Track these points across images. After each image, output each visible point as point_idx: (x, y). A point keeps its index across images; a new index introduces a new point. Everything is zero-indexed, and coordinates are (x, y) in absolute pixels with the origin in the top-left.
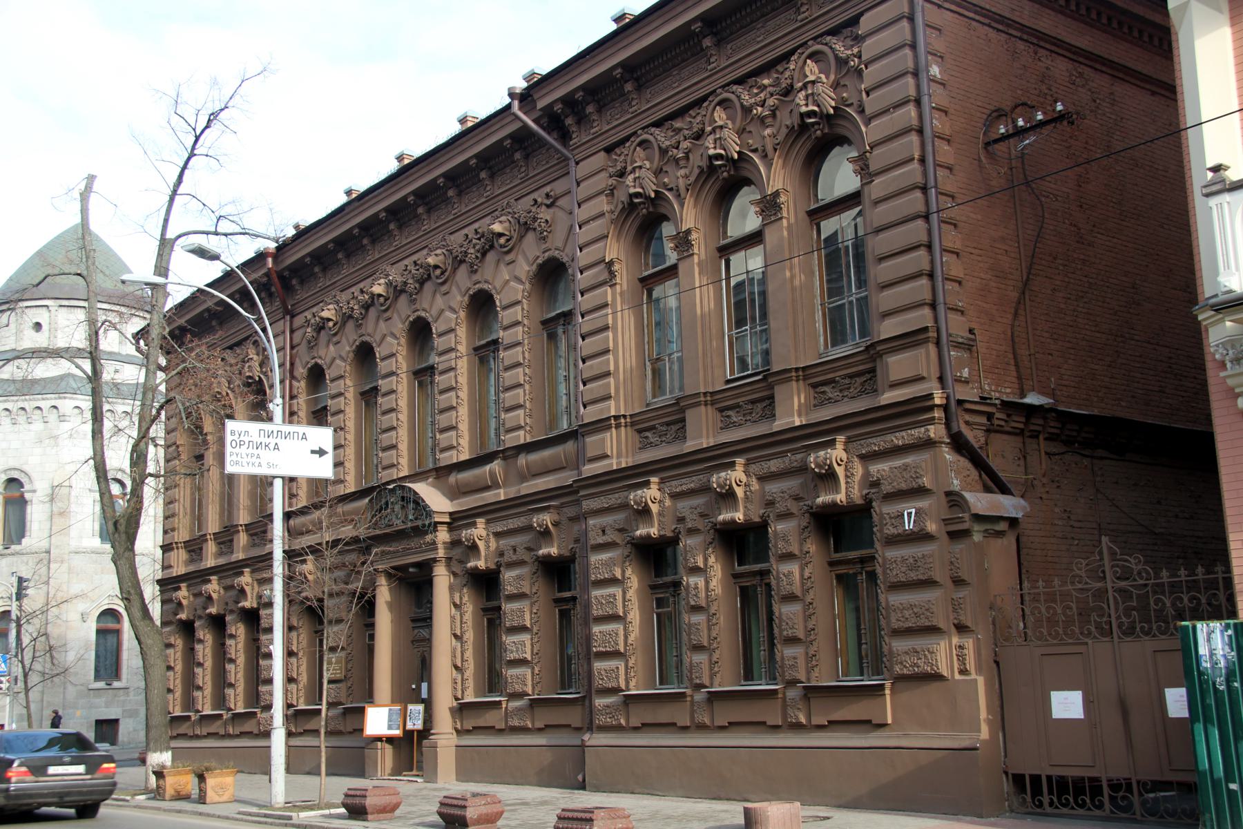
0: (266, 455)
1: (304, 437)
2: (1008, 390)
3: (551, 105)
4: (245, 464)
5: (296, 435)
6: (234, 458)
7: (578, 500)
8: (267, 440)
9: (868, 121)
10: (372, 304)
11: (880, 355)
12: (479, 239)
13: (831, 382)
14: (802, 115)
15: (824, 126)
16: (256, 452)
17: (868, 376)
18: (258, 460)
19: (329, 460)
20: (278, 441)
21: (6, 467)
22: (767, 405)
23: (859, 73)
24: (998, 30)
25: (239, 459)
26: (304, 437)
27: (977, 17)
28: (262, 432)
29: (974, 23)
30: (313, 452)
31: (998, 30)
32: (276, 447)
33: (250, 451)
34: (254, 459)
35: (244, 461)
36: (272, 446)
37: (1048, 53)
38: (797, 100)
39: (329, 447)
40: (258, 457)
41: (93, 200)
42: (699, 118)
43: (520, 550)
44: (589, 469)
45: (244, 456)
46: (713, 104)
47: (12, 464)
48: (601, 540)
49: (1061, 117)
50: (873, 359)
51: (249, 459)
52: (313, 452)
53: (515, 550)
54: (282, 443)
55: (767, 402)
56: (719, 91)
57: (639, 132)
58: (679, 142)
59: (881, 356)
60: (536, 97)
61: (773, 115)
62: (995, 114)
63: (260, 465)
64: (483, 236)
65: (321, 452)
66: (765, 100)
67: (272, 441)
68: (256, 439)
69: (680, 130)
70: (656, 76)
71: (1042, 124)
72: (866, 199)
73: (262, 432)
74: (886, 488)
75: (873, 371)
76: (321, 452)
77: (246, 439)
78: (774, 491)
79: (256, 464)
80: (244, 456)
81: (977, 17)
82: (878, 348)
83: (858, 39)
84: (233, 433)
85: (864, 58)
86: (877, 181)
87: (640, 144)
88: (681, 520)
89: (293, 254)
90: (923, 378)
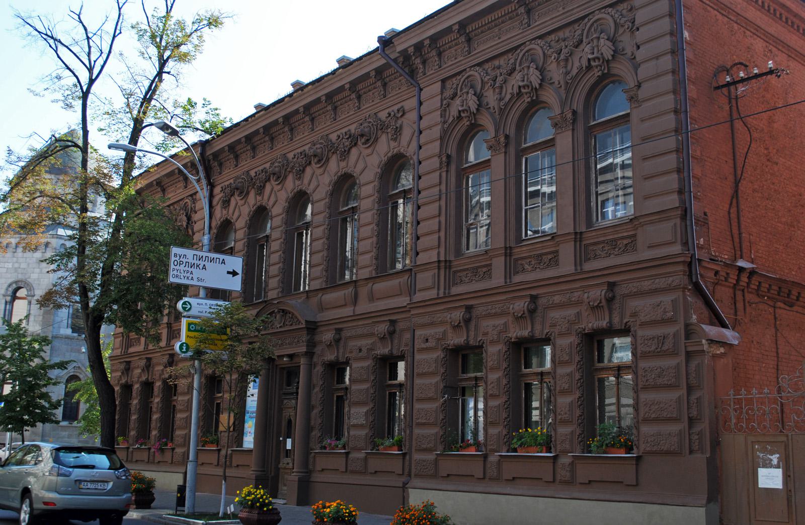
0: (197, 273)
1: (223, 262)
2: (726, 257)
3: (406, 50)
4: (182, 277)
5: (218, 260)
6: (175, 272)
7: (410, 317)
8: (198, 262)
10: (269, 180)
12: (348, 139)
15: (604, 69)
16: (190, 270)
18: (191, 275)
19: (238, 278)
20: (206, 263)
21: (16, 279)
24: (723, 14)
25: (179, 273)
26: (223, 262)
27: (711, 4)
28: (195, 256)
29: (709, 8)
30: (229, 273)
31: (723, 14)
32: (204, 267)
33: (186, 268)
34: (189, 274)
35: (182, 275)
36: (201, 267)
37: (752, 34)
38: (586, 50)
39: (239, 270)
40: (192, 273)
41: (91, 97)
43: (364, 350)
44: (419, 297)
45: (182, 271)
46: (523, 52)
47: (20, 277)
48: (424, 346)
49: (771, 72)
51: (185, 275)
52: (229, 273)
53: (360, 350)
54: (208, 264)
56: (528, 43)
57: (468, 70)
58: (497, 77)
60: (396, 43)
62: (720, 69)
63: (192, 279)
64: (350, 136)
65: (234, 273)
67: (202, 263)
68: (191, 260)
70: (482, 32)
71: (757, 76)
72: (634, 118)
73: (195, 256)
74: (643, 318)
76: (234, 273)
77: (184, 260)
78: (557, 317)
80: (182, 271)
81: (711, 4)
82: (641, 221)
84: (175, 255)
86: (645, 105)
88: (485, 334)
89: (218, 145)
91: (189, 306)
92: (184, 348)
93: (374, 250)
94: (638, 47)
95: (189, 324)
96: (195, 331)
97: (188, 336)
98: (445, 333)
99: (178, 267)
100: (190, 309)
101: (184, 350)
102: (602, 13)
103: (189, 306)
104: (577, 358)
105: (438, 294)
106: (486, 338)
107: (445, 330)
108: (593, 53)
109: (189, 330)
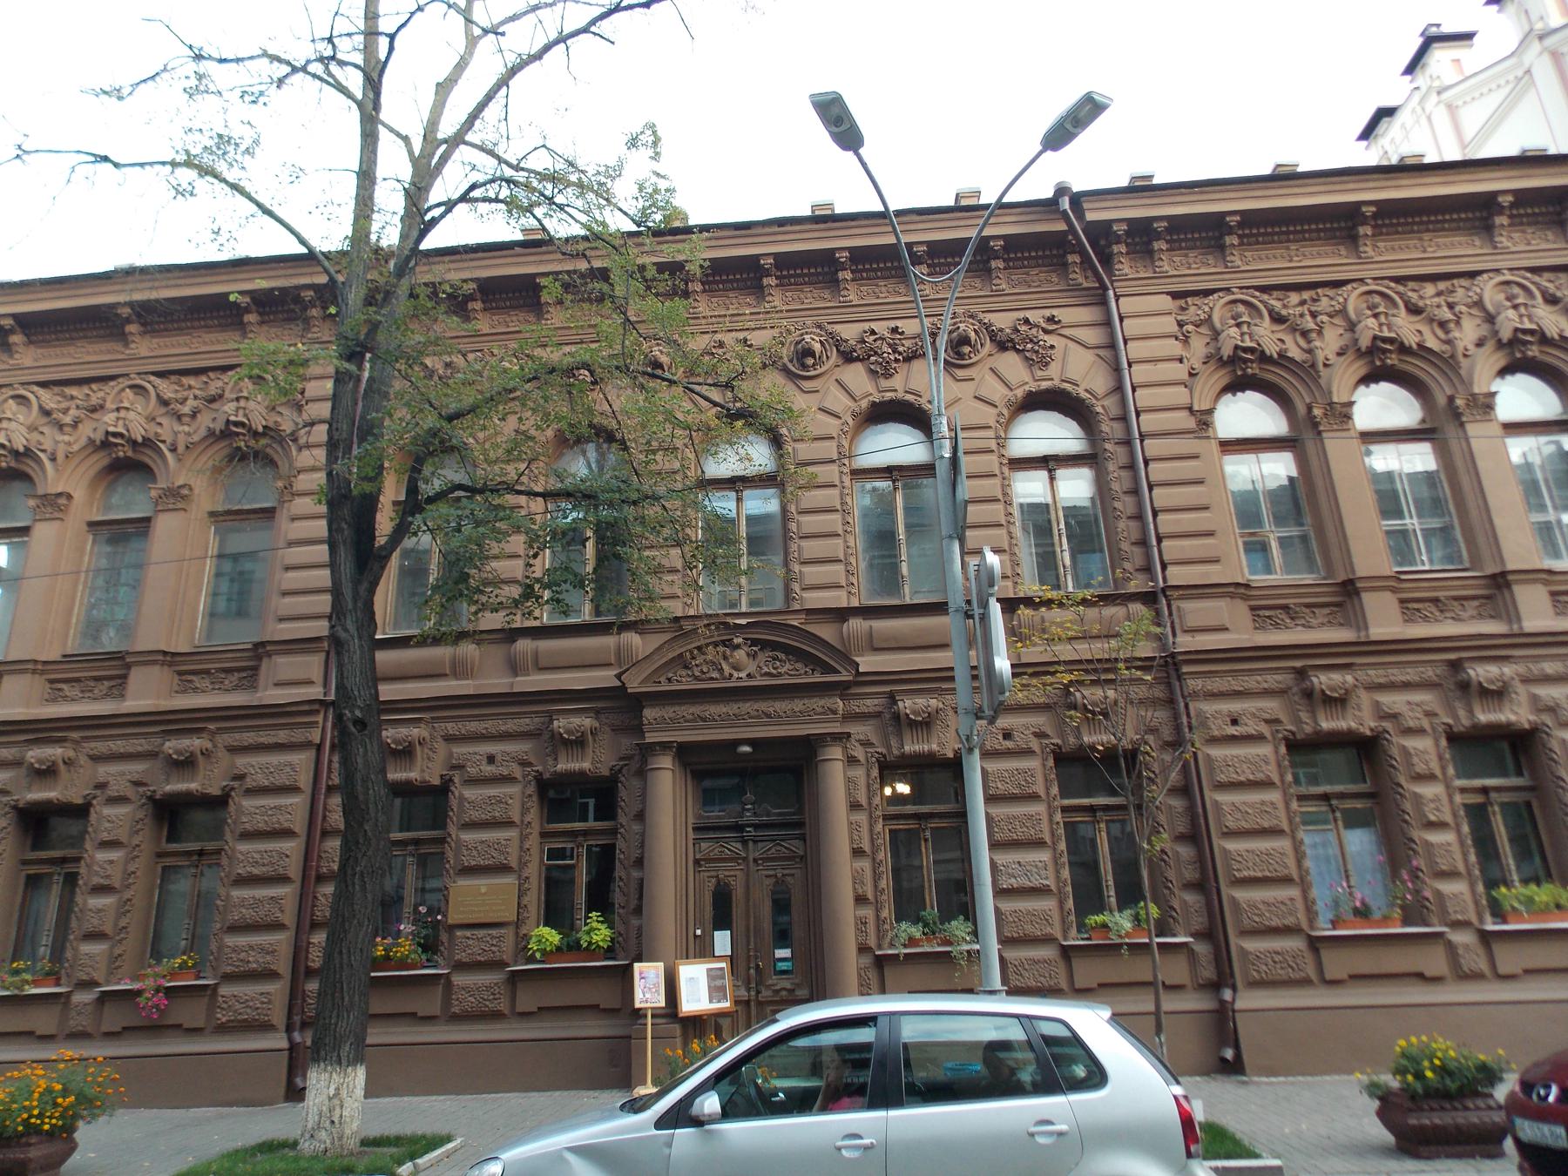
9: (300, 449)
11: (269, 655)
13: (207, 672)
17: (250, 673)
22: (119, 684)
23: (299, 408)
42: (101, 394)
50: (259, 658)
59: (270, 656)
61: (194, 415)
66: (186, 399)
69: (72, 398)
75: (256, 669)
83: (304, 379)
85: (306, 394)
86: (298, 501)
87: (13, 397)
90: (313, 682)
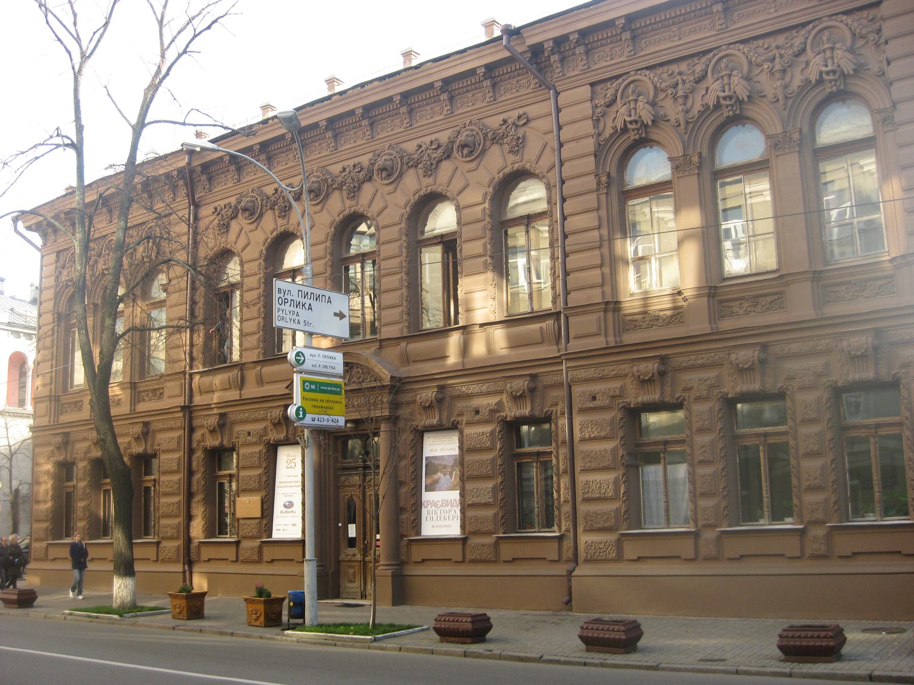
8: (303, 300)
14: (821, 73)
16: (296, 310)
20: (311, 301)
25: (284, 315)
30: (336, 314)
32: (310, 308)
33: (292, 308)
36: (307, 306)
52: (336, 314)
54: (314, 304)
55: (776, 297)
56: (723, 47)
63: (299, 323)
67: (307, 301)
68: (295, 298)
76: (341, 316)
77: (289, 298)
79: (296, 321)
84: (279, 290)
88: (688, 389)
91: (302, 359)
92: (301, 413)
93: (405, 304)
94: (889, 63)
95: (304, 382)
96: (311, 390)
97: (304, 398)
98: (500, 404)
99: (282, 307)
100: (304, 361)
101: (301, 416)
102: (832, 20)
103: (303, 359)
104: (621, 434)
105: (607, 342)
106: (687, 395)
107: (622, 386)
108: (827, 66)
109: (304, 390)
